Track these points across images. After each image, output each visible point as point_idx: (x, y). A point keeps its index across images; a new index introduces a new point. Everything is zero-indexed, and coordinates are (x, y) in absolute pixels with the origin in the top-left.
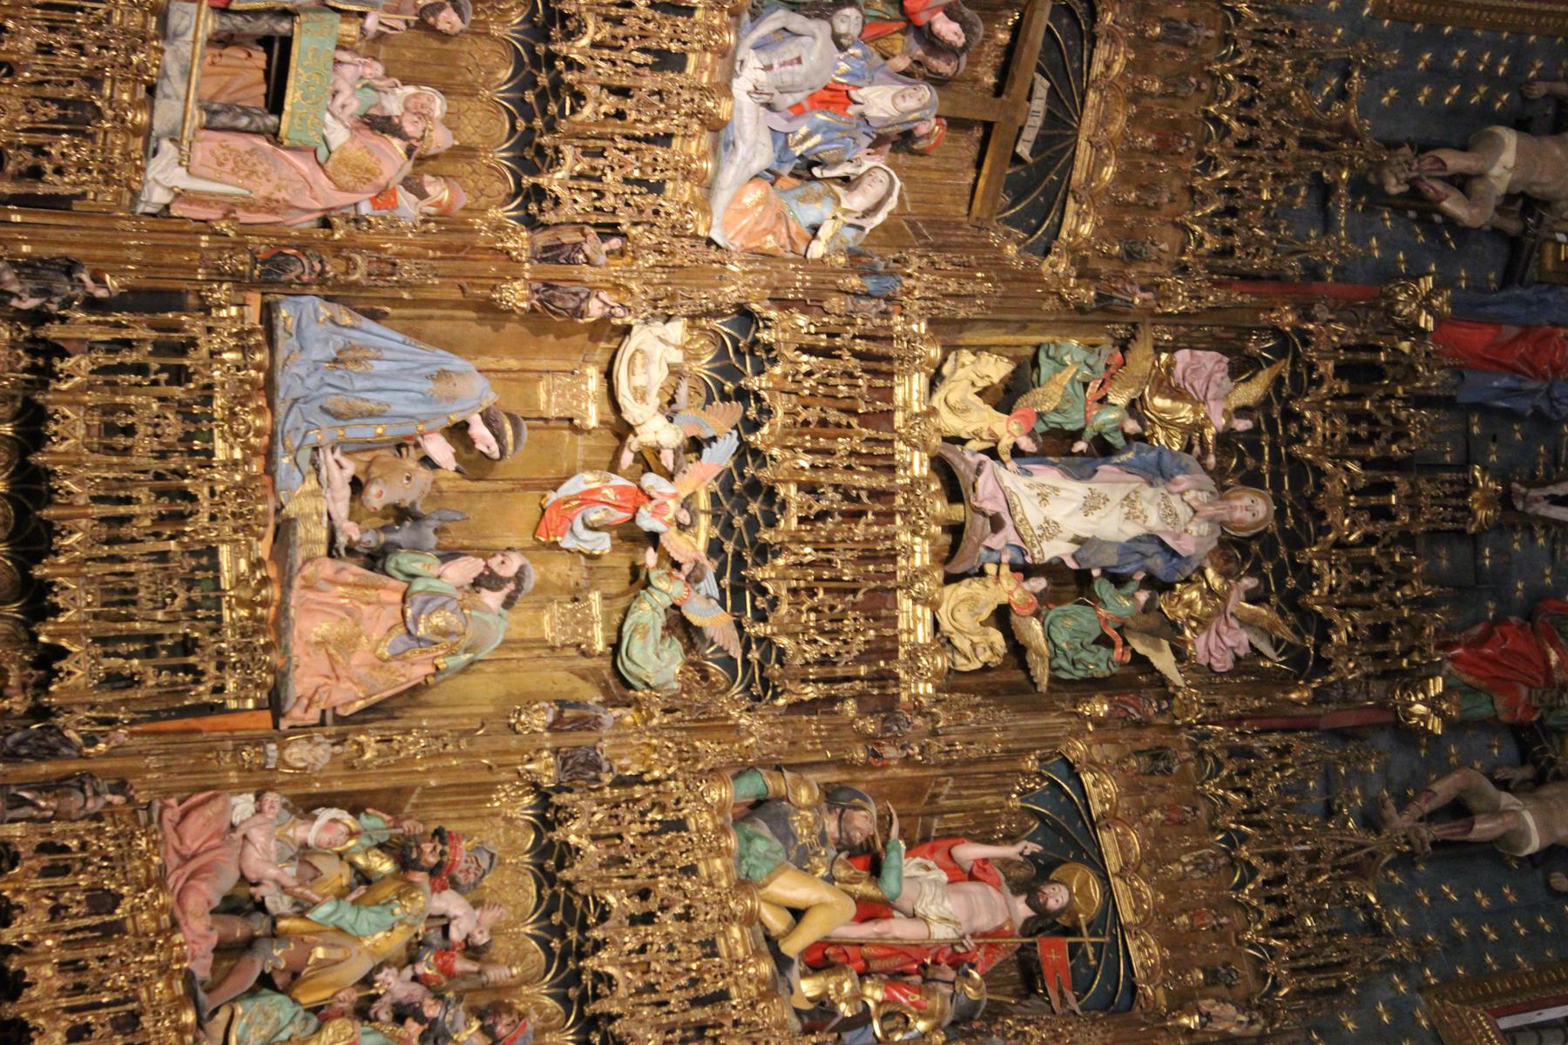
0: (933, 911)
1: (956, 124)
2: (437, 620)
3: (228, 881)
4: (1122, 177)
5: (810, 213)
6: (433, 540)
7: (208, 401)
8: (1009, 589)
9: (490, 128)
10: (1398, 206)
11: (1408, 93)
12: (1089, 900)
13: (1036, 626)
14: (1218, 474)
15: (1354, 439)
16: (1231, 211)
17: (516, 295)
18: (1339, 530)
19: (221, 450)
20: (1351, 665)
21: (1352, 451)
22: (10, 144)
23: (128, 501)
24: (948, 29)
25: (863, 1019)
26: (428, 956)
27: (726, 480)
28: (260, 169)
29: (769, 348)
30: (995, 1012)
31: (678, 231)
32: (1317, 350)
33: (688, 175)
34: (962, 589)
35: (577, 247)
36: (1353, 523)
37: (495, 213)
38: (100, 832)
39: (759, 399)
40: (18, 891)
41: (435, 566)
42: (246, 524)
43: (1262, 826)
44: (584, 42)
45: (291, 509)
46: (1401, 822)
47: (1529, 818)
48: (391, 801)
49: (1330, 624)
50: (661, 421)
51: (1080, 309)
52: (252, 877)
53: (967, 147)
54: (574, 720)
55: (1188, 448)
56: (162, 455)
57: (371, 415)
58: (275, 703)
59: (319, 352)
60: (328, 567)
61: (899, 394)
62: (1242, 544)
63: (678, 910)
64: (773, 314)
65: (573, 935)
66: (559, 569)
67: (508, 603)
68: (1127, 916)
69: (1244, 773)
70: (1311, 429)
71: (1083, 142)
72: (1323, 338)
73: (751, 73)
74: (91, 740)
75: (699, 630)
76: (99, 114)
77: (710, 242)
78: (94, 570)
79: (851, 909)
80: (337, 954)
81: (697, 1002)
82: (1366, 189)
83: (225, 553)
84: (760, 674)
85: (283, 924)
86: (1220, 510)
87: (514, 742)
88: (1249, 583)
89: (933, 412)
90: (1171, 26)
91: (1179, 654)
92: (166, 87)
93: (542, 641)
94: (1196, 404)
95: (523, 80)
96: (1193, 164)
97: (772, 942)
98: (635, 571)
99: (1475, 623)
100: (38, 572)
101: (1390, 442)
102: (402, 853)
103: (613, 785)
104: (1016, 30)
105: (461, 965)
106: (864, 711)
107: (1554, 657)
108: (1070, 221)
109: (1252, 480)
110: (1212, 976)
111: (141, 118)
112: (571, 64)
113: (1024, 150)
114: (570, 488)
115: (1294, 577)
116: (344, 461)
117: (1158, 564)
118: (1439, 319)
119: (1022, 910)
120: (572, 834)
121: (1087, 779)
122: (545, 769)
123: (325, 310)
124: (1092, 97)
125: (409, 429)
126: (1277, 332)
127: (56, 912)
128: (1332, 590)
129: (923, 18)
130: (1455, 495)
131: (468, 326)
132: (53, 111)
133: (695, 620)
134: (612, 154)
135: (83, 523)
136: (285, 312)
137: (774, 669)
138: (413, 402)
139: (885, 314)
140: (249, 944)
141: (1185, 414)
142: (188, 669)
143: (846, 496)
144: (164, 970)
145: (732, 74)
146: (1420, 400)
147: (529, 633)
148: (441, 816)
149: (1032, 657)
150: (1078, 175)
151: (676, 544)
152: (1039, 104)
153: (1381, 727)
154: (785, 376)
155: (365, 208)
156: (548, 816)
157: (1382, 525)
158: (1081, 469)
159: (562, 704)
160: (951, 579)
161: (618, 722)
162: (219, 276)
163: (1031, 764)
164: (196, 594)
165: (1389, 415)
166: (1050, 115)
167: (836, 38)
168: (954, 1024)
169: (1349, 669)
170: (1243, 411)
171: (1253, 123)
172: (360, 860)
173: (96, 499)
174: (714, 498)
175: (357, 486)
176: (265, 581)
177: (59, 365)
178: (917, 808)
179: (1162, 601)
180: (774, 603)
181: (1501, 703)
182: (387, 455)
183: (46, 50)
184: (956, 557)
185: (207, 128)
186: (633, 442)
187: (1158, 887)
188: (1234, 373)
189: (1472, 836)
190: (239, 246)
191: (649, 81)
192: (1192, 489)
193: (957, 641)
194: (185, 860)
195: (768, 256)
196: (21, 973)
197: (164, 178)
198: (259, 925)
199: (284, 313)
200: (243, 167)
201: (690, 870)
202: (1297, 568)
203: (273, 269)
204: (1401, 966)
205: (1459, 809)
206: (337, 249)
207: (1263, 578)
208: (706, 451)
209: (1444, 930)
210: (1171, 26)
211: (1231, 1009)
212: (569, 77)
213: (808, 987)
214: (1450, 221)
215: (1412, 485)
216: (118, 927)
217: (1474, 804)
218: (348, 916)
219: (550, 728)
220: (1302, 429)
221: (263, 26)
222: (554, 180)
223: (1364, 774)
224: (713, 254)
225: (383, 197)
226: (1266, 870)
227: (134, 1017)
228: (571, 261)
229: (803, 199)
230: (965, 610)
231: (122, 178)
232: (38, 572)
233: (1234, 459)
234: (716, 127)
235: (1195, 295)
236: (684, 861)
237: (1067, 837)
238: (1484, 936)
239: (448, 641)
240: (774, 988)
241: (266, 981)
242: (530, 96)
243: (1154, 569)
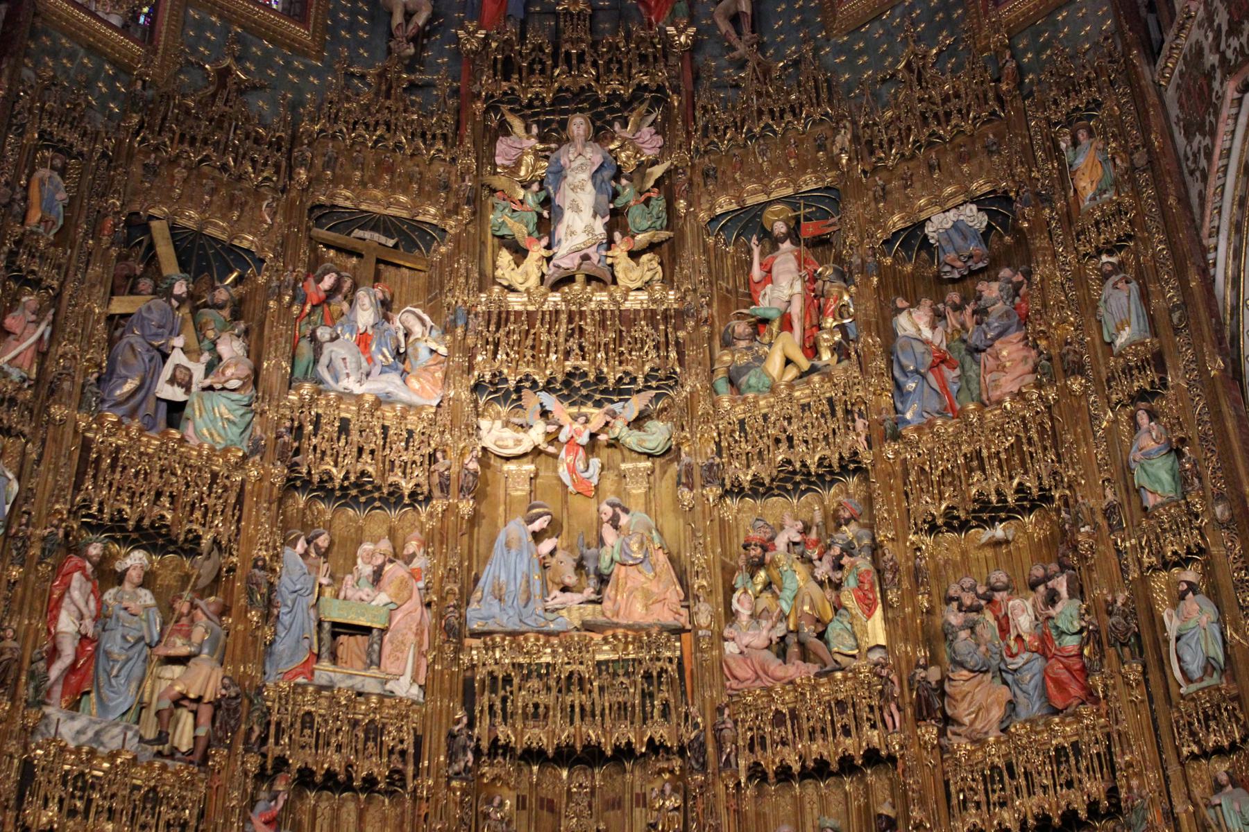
0: (787, 292)
1: (377, 278)
2: (635, 547)
3: (769, 656)
4: (405, 192)
5: (423, 354)
6: (593, 550)
7: (521, 666)
8: (620, 252)
9: (381, 519)
10: (421, 48)
11: (362, 43)
12: (781, 211)
13: (639, 237)
14: (561, 142)
15: (542, 72)
16: (423, 135)
17: (466, 507)
19: (546, 659)
21: (549, 73)
22: (388, 766)
23: (572, 706)
24: (328, 281)
25: (842, 328)
26: (808, 552)
27: (563, 398)
28: (400, 638)
29: (494, 375)
30: (839, 259)
31: (432, 423)
33: (403, 417)
34: (620, 275)
35: (441, 475)
37: (423, 518)
38: (743, 721)
39: (520, 381)
40: (773, 762)
41: (608, 548)
42: (585, 646)
43: (743, 121)
44: (334, 470)
45: (577, 623)
46: (741, 49)
48: (728, 572)
49: (639, 85)
50: (532, 431)
51: (474, 213)
52: (767, 643)
53: (389, 272)
54: (687, 477)
55: (547, 158)
56: (549, 689)
57: (528, 582)
58: (678, 631)
59: (496, 609)
60: (607, 604)
61: (518, 308)
62: (597, 130)
63: (786, 423)
64: (476, 373)
65: (798, 478)
66: (609, 484)
67: (626, 511)
68: (790, 191)
69: (716, 129)
70: (537, 94)
71: (387, 212)
73: (350, 384)
74: (696, 725)
75: (641, 412)
76: (372, 721)
77: (439, 406)
78: (608, 724)
79: (786, 334)
80: (807, 599)
81: (833, 413)
82: (412, 64)
83: (599, 657)
84: (664, 381)
85: (791, 627)
86: (579, 141)
87: (698, 508)
88: (617, 127)
89: (527, 290)
90: (327, 165)
91: (654, 163)
92: (358, 687)
93: (646, 494)
94: (524, 153)
95: (355, 502)
96: (399, 155)
97: (803, 375)
98: (610, 445)
99: (638, 10)
100: (609, 753)
102: (756, 566)
103: (721, 457)
104: (328, 246)
105: (813, 536)
106: (683, 327)
108: (428, 219)
109: (563, 125)
110: (821, 147)
111: (374, 699)
112: (346, 478)
113: (391, 243)
114: (566, 479)
116: (552, 596)
117: (607, 174)
118: (480, 27)
119: (786, 246)
120: (746, 478)
121: (719, 211)
122: (713, 492)
123: (474, 605)
124: (363, 207)
125: (536, 562)
126: (486, 112)
127: (784, 743)
128: (621, 84)
129: (322, 295)
130: (572, 20)
131: (482, 531)
132: (371, 744)
133: (635, 415)
134: (393, 456)
135: (584, 729)
136: (475, 626)
137: (661, 373)
138: (522, 559)
139: (476, 315)
140: (801, 644)
141: (529, 159)
142: (659, 676)
143: (571, 335)
144: (814, 688)
145: (351, 394)
146: (522, 37)
147: (642, 501)
148: (737, 546)
149: (656, 240)
150: (404, 214)
151: (595, 425)
152: (367, 235)
153: (692, 58)
154: (508, 367)
155: (421, 584)
156: (737, 491)
157: (588, 58)
158: (557, 213)
159: (679, 483)
160: (615, 282)
161: (688, 454)
162: (456, 660)
163: (711, 240)
164: (621, 672)
165: (530, 54)
166: (373, 229)
167: (333, 340)
168: (845, 281)
169: (662, 75)
170: (528, 129)
171: (377, 123)
172: (759, 588)
173: (572, 723)
174: (572, 404)
175: (565, 589)
176: (615, 636)
177: (502, 742)
178: (733, 299)
179: (626, 172)
180: (627, 373)
182: (549, 574)
183: (339, 748)
184: (603, 279)
185: (379, 665)
186: (543, 446)
187: (775, 175)
188: (507, 134)
189: (749, 12)
190: (440, 650)
191: (355, 437)
192: (568, 156)
193: (647, 278)
194: (758, 677)
195: (446, 376)
196: (816, 760)
197: (406, 688)
198: (792, 639)
199: (475, 626)
200: (400, 647)
201: (765, 417)
202: (609, 102)
203: (452, 631)
204: (816, 50)
205: (735, 19)
206: (442, 599)
207: (615, 119)
208: (548, 408)
209: (797, 28)
210: (327, 165)
211: (838, 138)
212: (353, 479)
213: (826, 356)
214: (429, 21)
216: (793, 712)
217: (732, 12)
218: (788, 594)
219: (691, 490)
220: (537, 99)
221: (326, 636)
222: (407, 486)
223: (718, 68)
224: (445, 404)
225: (415, 575)
226: (766, 119)
227: (838, 703)
228: (448, 478)
229: (416, 357)
230: (630, 274)
231: (404, 709)
232: (609, 753)
233: (553, 134)
234: (378, 403)
235: (467, 154)
236: (761, 421)
237: (749, 222)
238: (801, 7)
239: (646, 542)
240: (827, 375)
241: (821, 636)
242: (363, 499)
243: (610, 176)
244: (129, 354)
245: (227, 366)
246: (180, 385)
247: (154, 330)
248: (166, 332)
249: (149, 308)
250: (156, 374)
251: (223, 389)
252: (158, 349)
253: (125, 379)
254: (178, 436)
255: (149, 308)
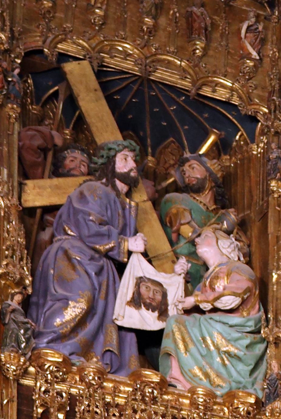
244: (63, 263)
245: (217, 277)
246: (148, 307)
247: (95, 228)
248: (115, 231)
249: (82, 196)
250: (111, 293)
251: (215, 310)
252: (106, 255)
253: (65, 302)
254: (156, 379)
255: (82, 196)
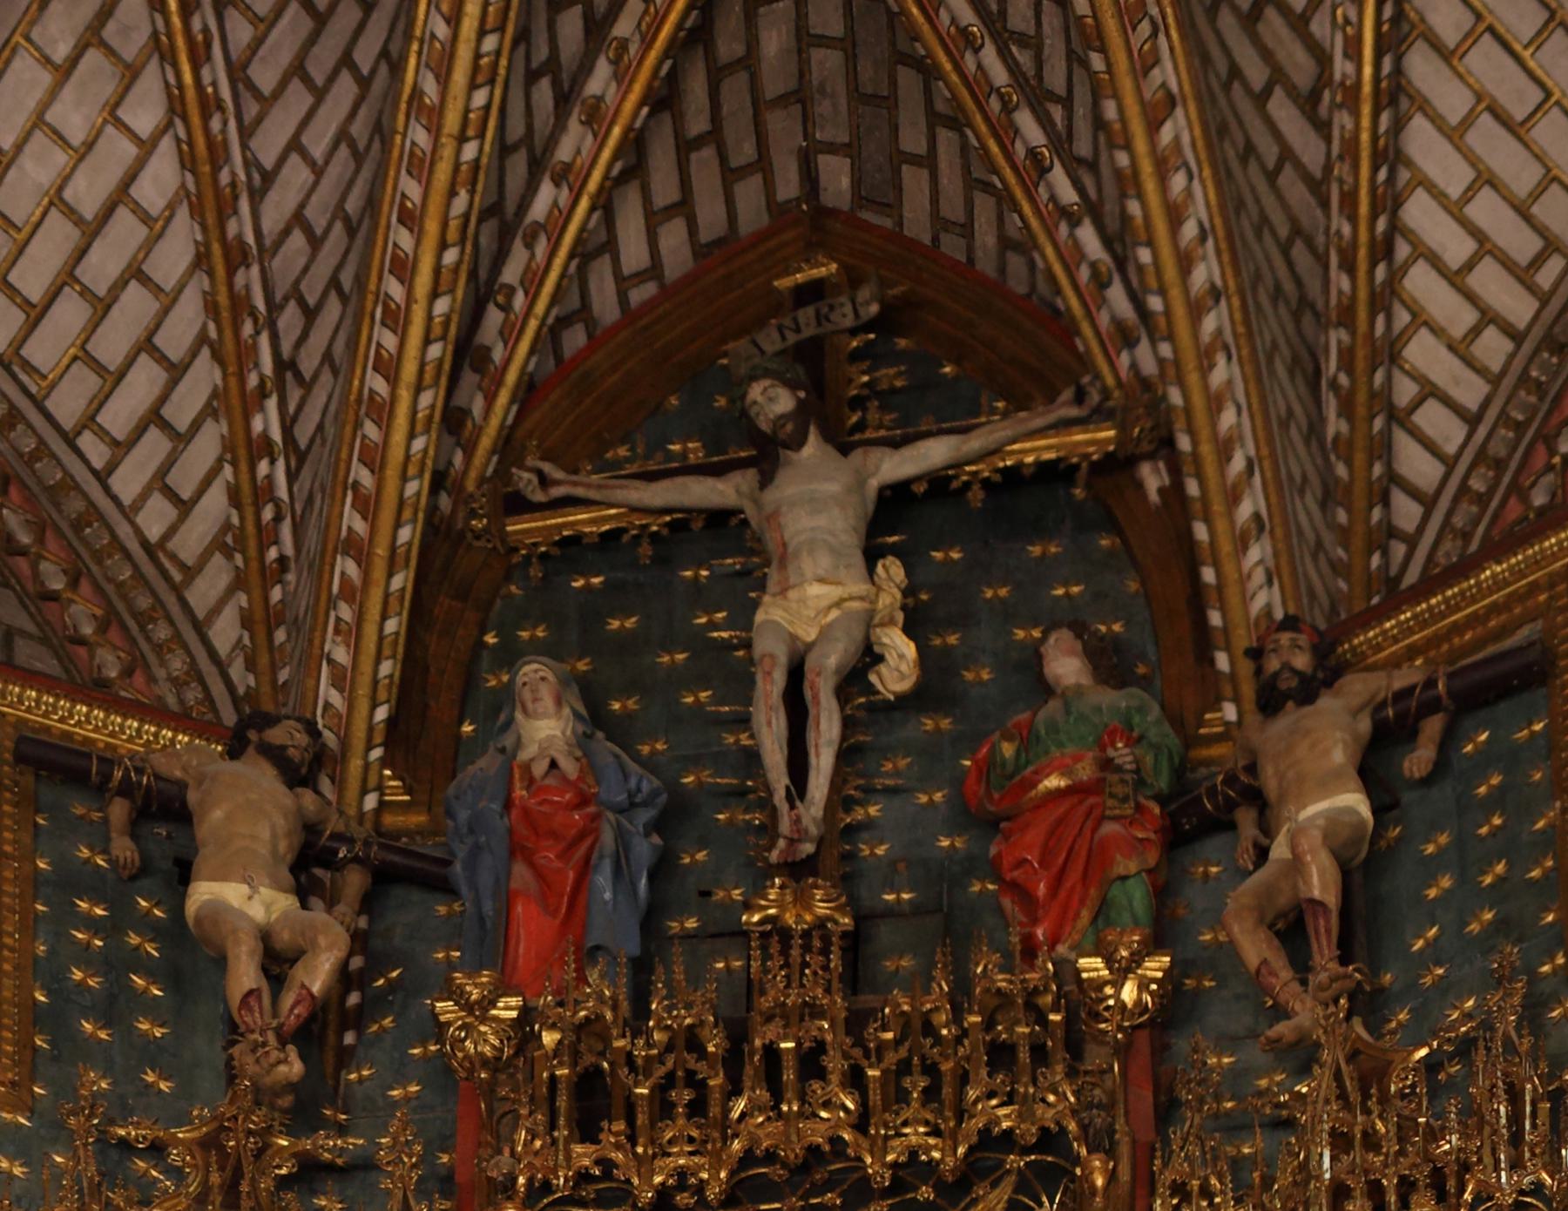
18: (838, 1124)
20: (1051, 1098)
21: (714, 1111)
32: (554, 1171)
36: (826, 1105)
47: (1311, 810)
49: (985, 1133)
72: (537, 1163)
99: (1000, 910)
101: (702, 1054)
107: (1053, 782)
115: (916, 1189)
128: (935, 1132)
130: (785, 952)
165: (660, 1059)
181: (1126, 865)
189: (1332, 900)
215: (769, 1019)
220: (682, 1186)
238: (1501, 880)
